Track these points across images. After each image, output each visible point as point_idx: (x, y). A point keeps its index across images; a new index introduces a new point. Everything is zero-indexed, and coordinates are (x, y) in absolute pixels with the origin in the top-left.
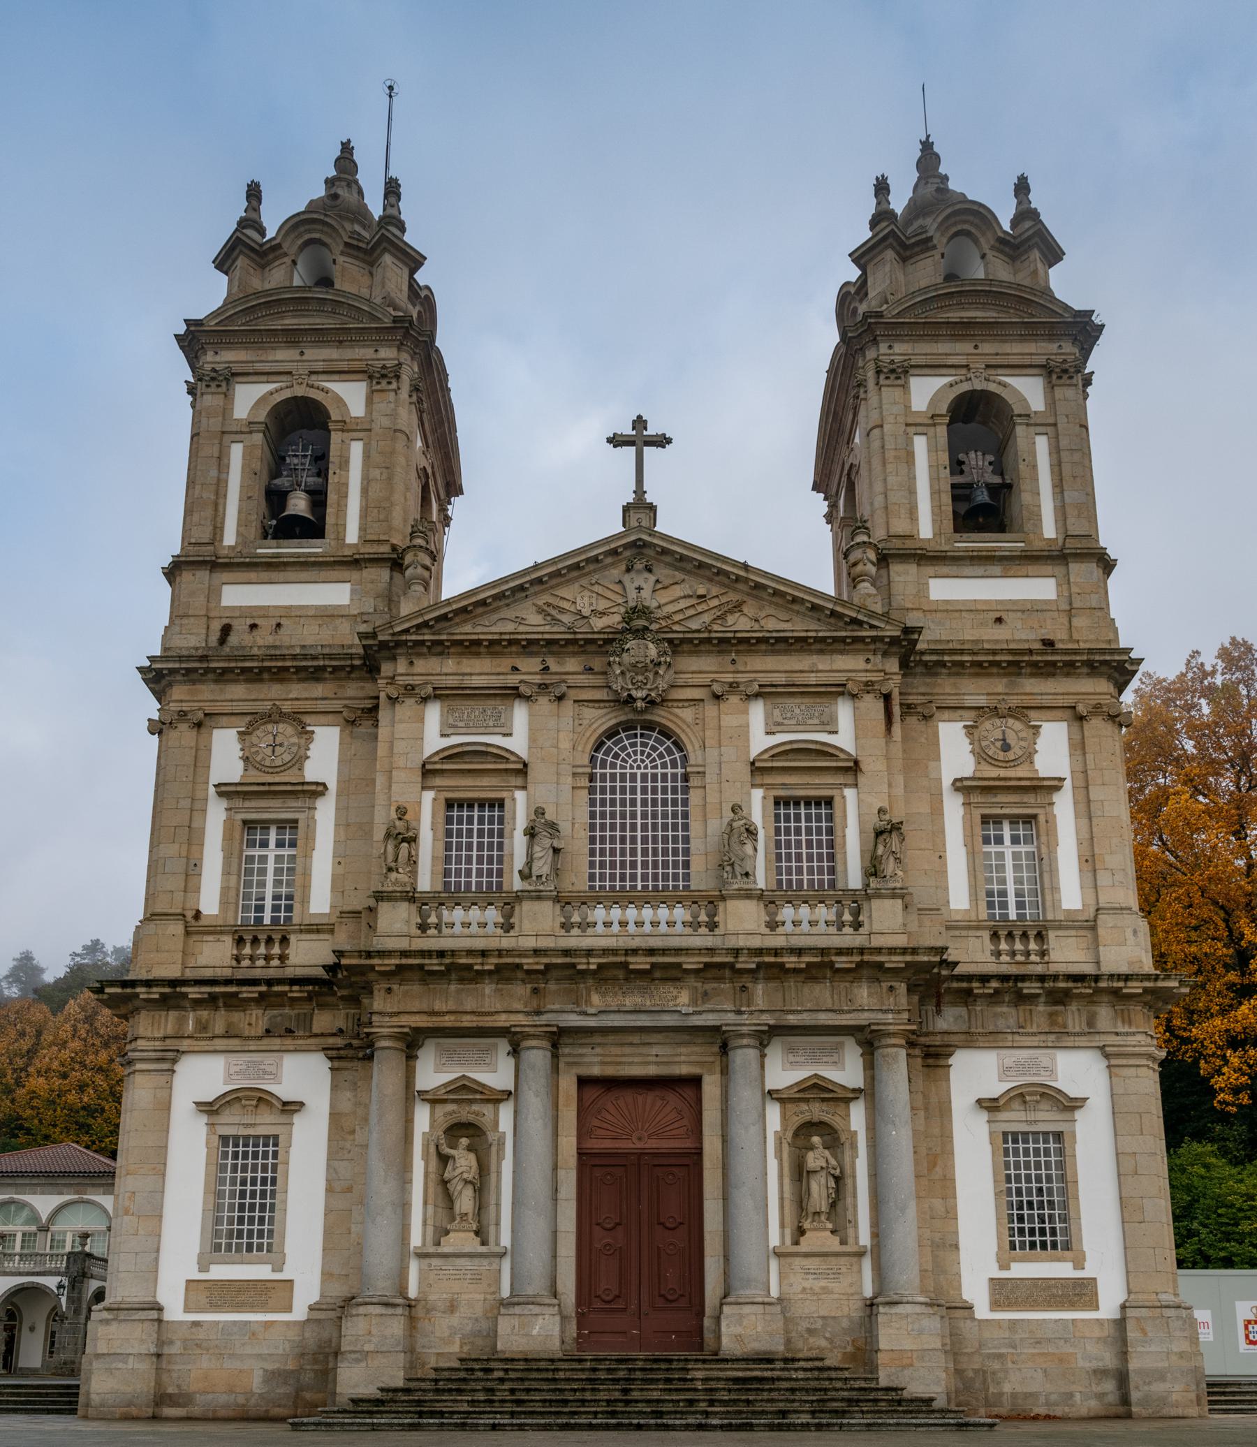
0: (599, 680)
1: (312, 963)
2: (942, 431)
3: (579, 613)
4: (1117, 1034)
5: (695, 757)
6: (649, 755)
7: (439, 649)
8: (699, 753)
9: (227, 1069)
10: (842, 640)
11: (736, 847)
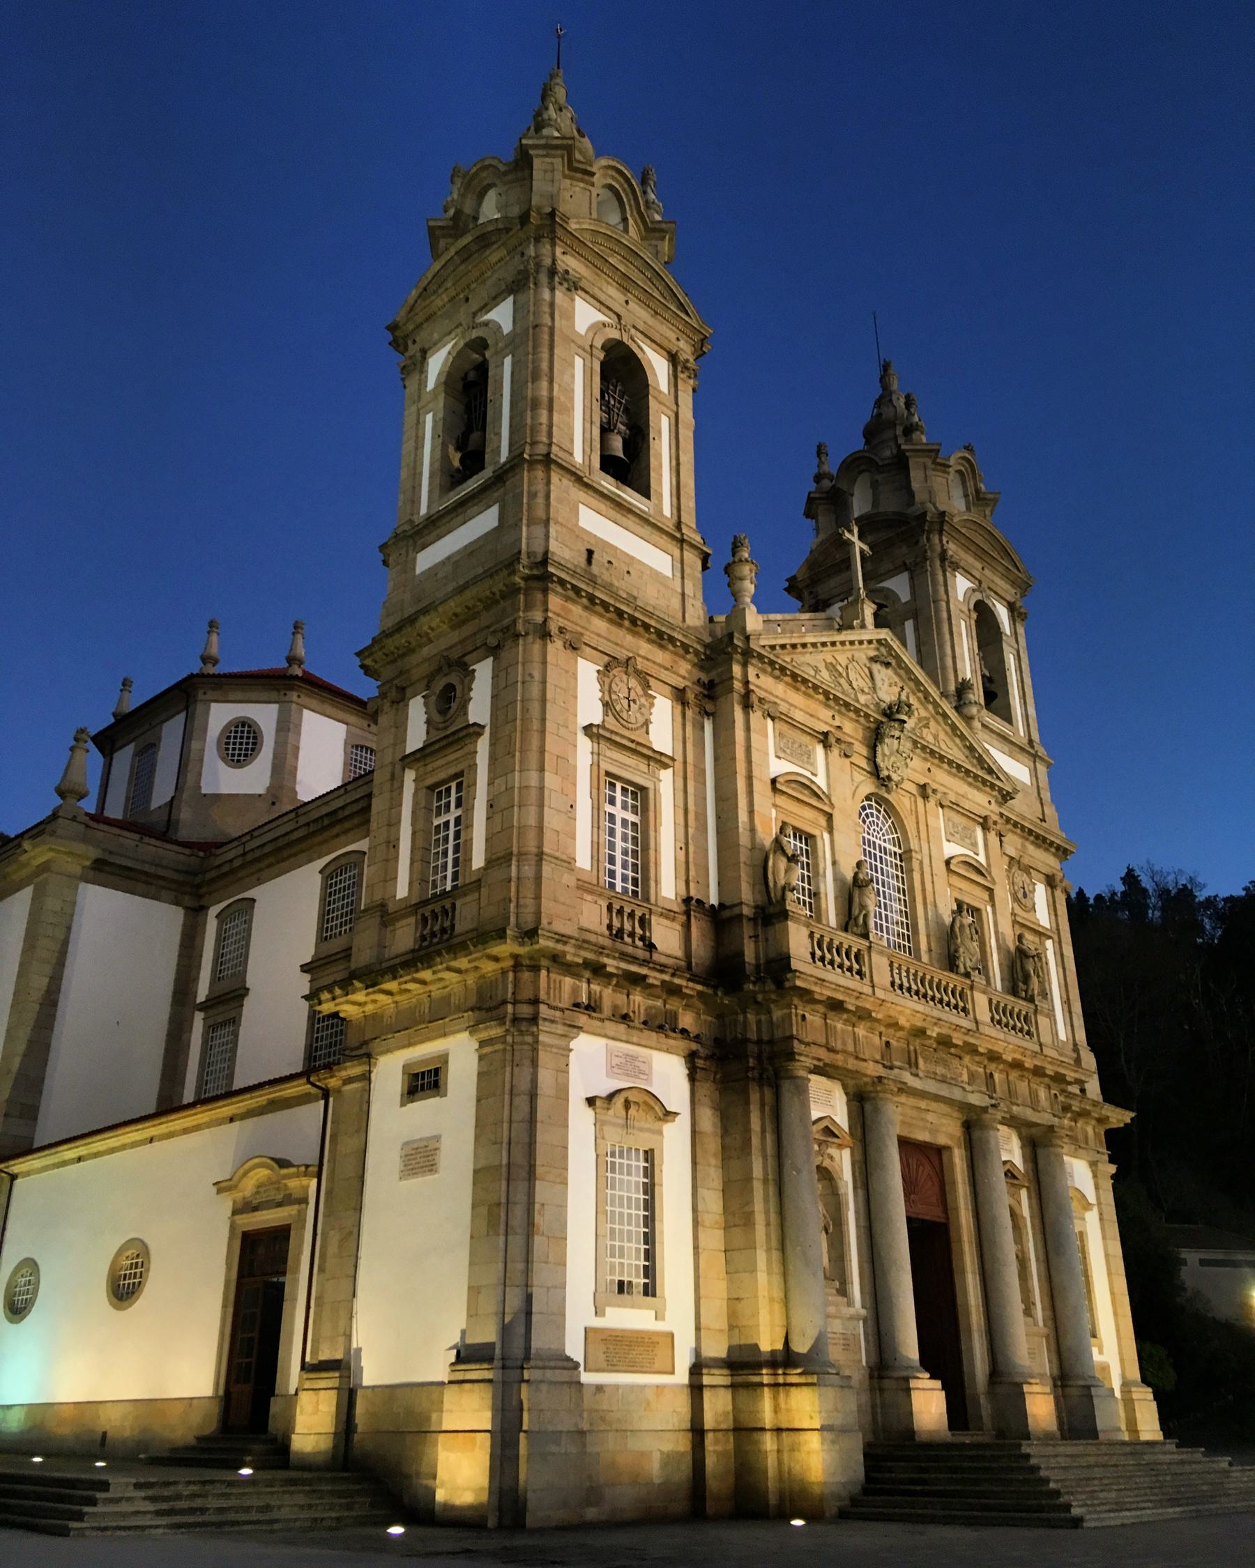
0: (864, 751)
1: (669, 952)
2: (973, 622)
3: (851, 684)
4: (1098, 1152)
5: (914, 844)
6: (881, 830)
7: (781, 671)
8: (916, 841)
9: (610, 1053)
10: (984, 782)
11: (968, 942)
